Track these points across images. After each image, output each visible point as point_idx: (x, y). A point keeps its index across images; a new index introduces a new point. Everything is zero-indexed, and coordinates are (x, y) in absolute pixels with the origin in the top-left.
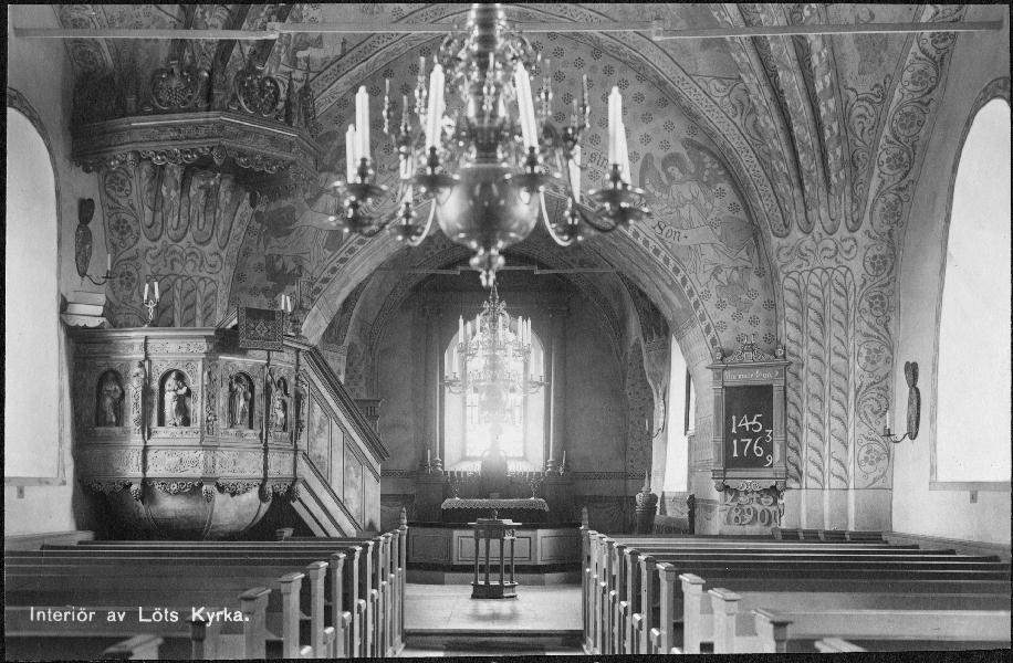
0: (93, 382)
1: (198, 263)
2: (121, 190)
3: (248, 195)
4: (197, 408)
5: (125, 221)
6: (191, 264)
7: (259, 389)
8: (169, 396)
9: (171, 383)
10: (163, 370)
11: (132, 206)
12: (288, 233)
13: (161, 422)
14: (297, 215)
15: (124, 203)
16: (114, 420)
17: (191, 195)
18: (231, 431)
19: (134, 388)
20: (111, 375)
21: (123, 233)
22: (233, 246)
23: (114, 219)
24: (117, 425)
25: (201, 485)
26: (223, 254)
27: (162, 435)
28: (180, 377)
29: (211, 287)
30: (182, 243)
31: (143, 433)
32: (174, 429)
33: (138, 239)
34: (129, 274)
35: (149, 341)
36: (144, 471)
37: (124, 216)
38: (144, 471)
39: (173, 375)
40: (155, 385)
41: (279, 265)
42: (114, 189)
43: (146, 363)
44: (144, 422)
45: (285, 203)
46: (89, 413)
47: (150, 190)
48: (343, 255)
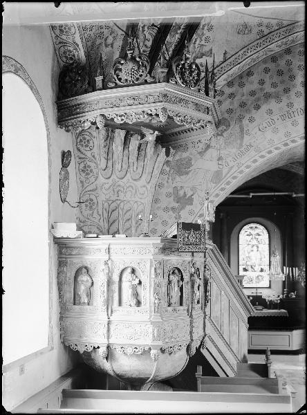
0: (71, 274)
1: (134, 191)
2: (87, 146)
3: (164, 149)
4: (147, 295)
5: (89, 167)
6: (129, 194)
7: (186, 278)
8: (126, 286)
9: (127, 276)
10: (122, 267)
11: (94, 156)
12: (187, 173)
13: (120, 304)
14: (193, 162)
15: (89, 154)
16: (86, 301)
17: (130, 149)
18: (169, 308)
19: (100, 279)
20: (84, 270)
21: (87, 174)
22: (154, 181)
23: (82, 165)
24: (89, 304)
25: (150, 349)
26: (148, 187)
27: (119, 314)
28: (133, 271)
29: (141, 208)
30: (125, 180)
31: (107, 312)
32: (131, 309)
33: (97, 177)
34: (92, 200)
35: (111, 247)
36: (108, 338)
37: (89, 163)
38: (108, 338)
39: (129, 270)
40: (116, 278)
41: (181, 193)
42: (82, 146)
43: (109, 262)
44: (108, 303)
45: (185, 155)
46: (69, 295)
47: (105, 146)
48: (223, 186)
